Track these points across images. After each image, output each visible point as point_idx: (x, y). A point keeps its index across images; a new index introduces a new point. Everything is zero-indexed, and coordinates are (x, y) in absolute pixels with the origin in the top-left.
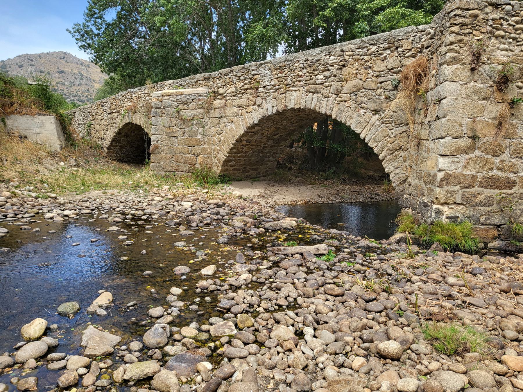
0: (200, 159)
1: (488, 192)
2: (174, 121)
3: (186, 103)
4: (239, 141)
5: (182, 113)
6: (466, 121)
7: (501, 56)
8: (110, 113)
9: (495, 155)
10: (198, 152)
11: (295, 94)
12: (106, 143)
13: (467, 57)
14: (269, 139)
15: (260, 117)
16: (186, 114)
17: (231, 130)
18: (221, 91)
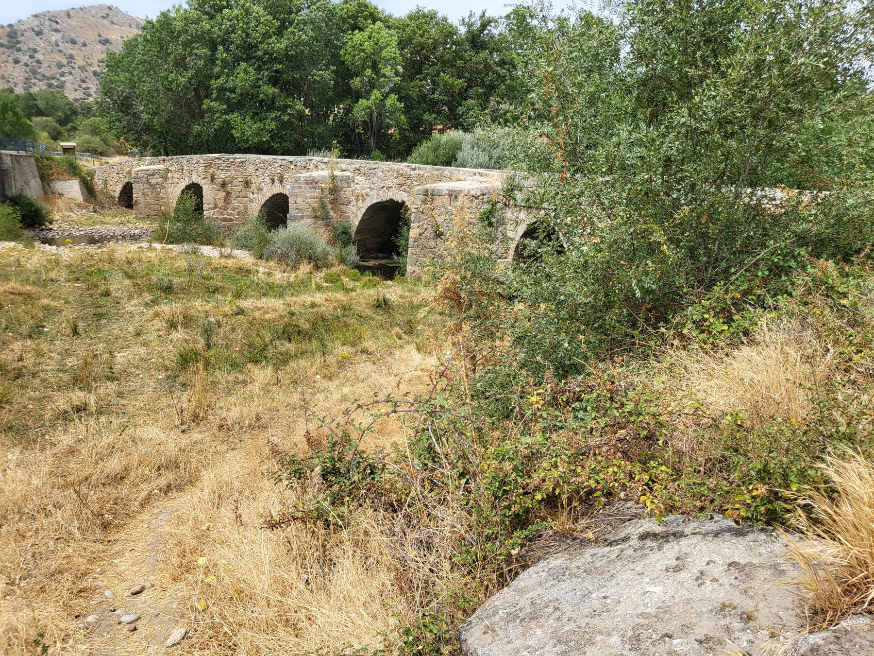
1: (223, 223)
3: (153, 175)
5: (150, 181)
7: (222, 176)
8: (118, 174)
9: (224, 210)
12: (117, 194)
16: (153, 181)
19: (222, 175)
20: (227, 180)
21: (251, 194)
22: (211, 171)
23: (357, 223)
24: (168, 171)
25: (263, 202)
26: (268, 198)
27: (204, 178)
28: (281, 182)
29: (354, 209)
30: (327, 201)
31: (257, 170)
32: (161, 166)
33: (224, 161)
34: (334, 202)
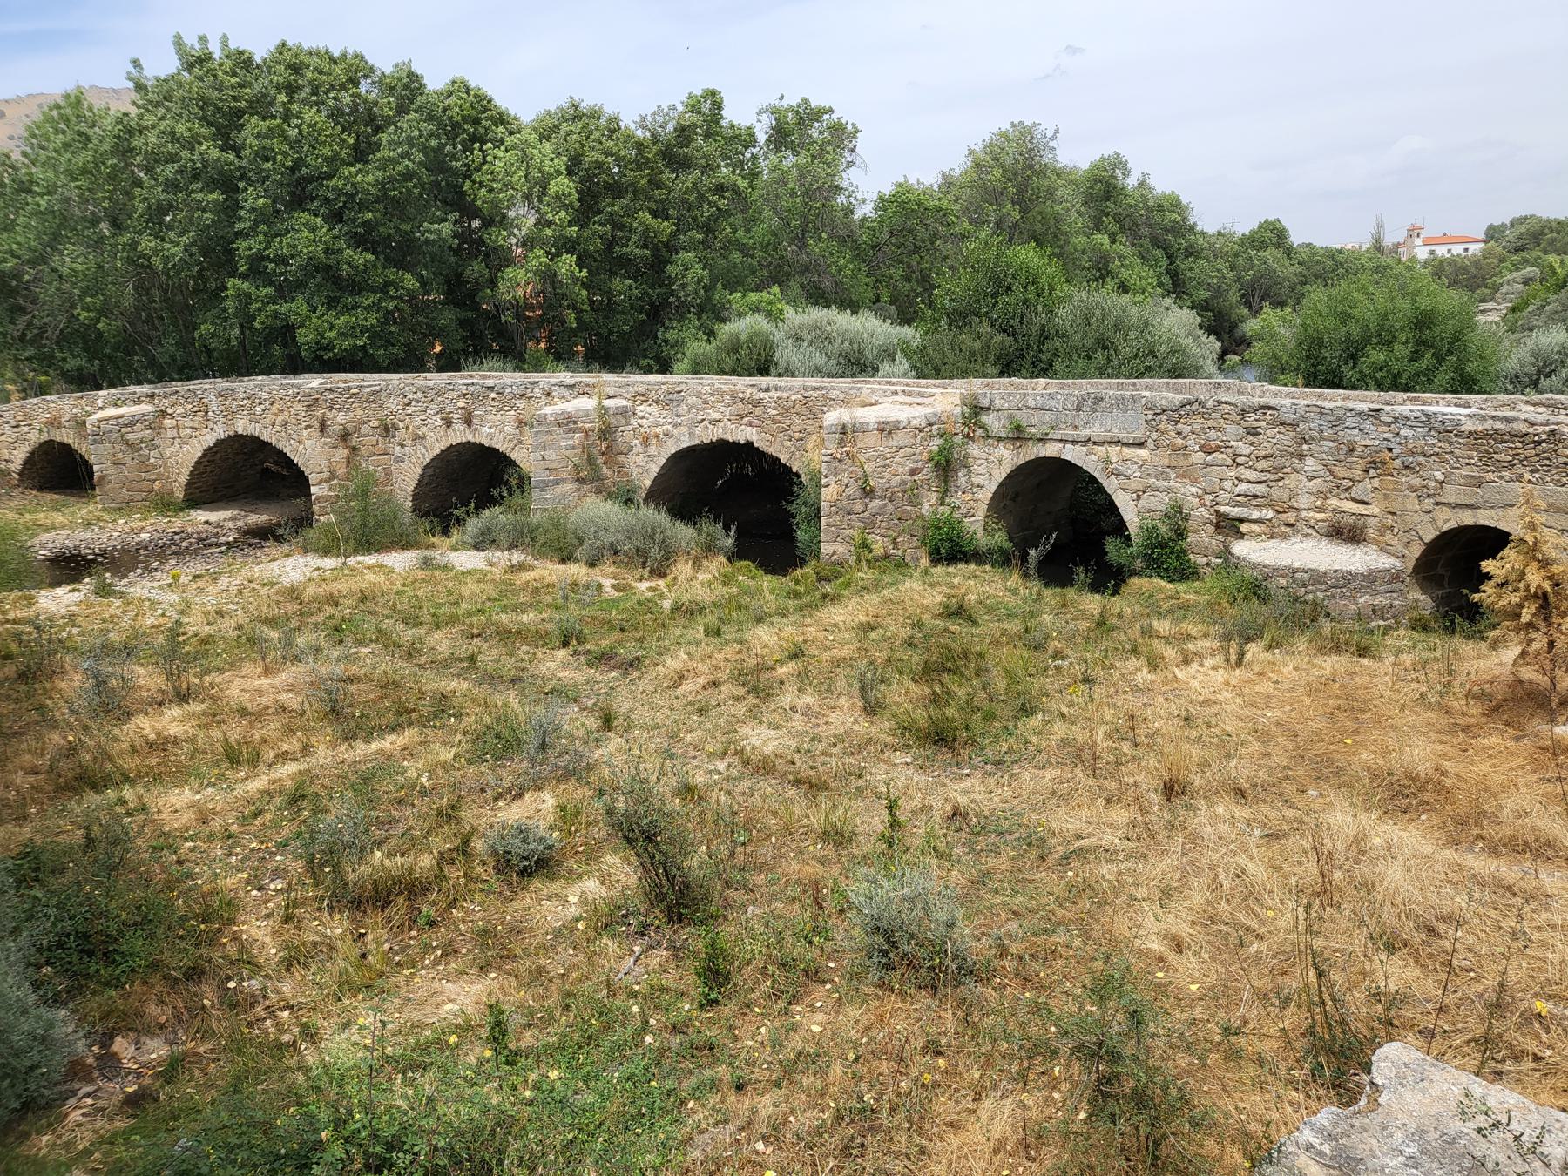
0: (157, 486)
2: (118, 448)
4: (198, 463)
6: (324, 463)
7: (340, 420)
8: (17, 426)
10: (154, 477)
11: (241, 422)
12: (16, 466)
13: (316, 424)
14: (237, 454)
15: (214, 440)
16: (132, 437)
17: (188, 452)
18: (169, 411)
19: (339, 420)
20: (349, 426)
21: (398, 448)
22: (319, 414)
23: (648, 483)
24: (164, 414)
25: (428, 460)
26: (438, 452)
27: (307, 427)
28: (469, 422)
29: (640, 459)
30: (594, 451)
31: (409, 404)
32: (144, 408)
33: (340, 393)
34: (609, 452)
